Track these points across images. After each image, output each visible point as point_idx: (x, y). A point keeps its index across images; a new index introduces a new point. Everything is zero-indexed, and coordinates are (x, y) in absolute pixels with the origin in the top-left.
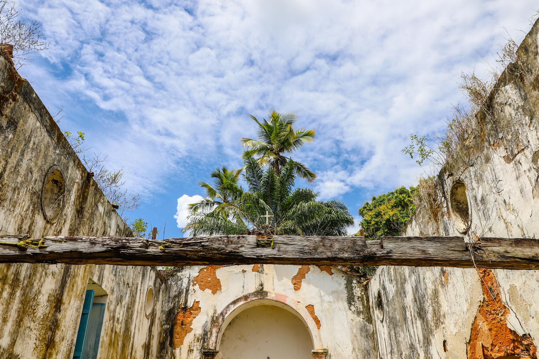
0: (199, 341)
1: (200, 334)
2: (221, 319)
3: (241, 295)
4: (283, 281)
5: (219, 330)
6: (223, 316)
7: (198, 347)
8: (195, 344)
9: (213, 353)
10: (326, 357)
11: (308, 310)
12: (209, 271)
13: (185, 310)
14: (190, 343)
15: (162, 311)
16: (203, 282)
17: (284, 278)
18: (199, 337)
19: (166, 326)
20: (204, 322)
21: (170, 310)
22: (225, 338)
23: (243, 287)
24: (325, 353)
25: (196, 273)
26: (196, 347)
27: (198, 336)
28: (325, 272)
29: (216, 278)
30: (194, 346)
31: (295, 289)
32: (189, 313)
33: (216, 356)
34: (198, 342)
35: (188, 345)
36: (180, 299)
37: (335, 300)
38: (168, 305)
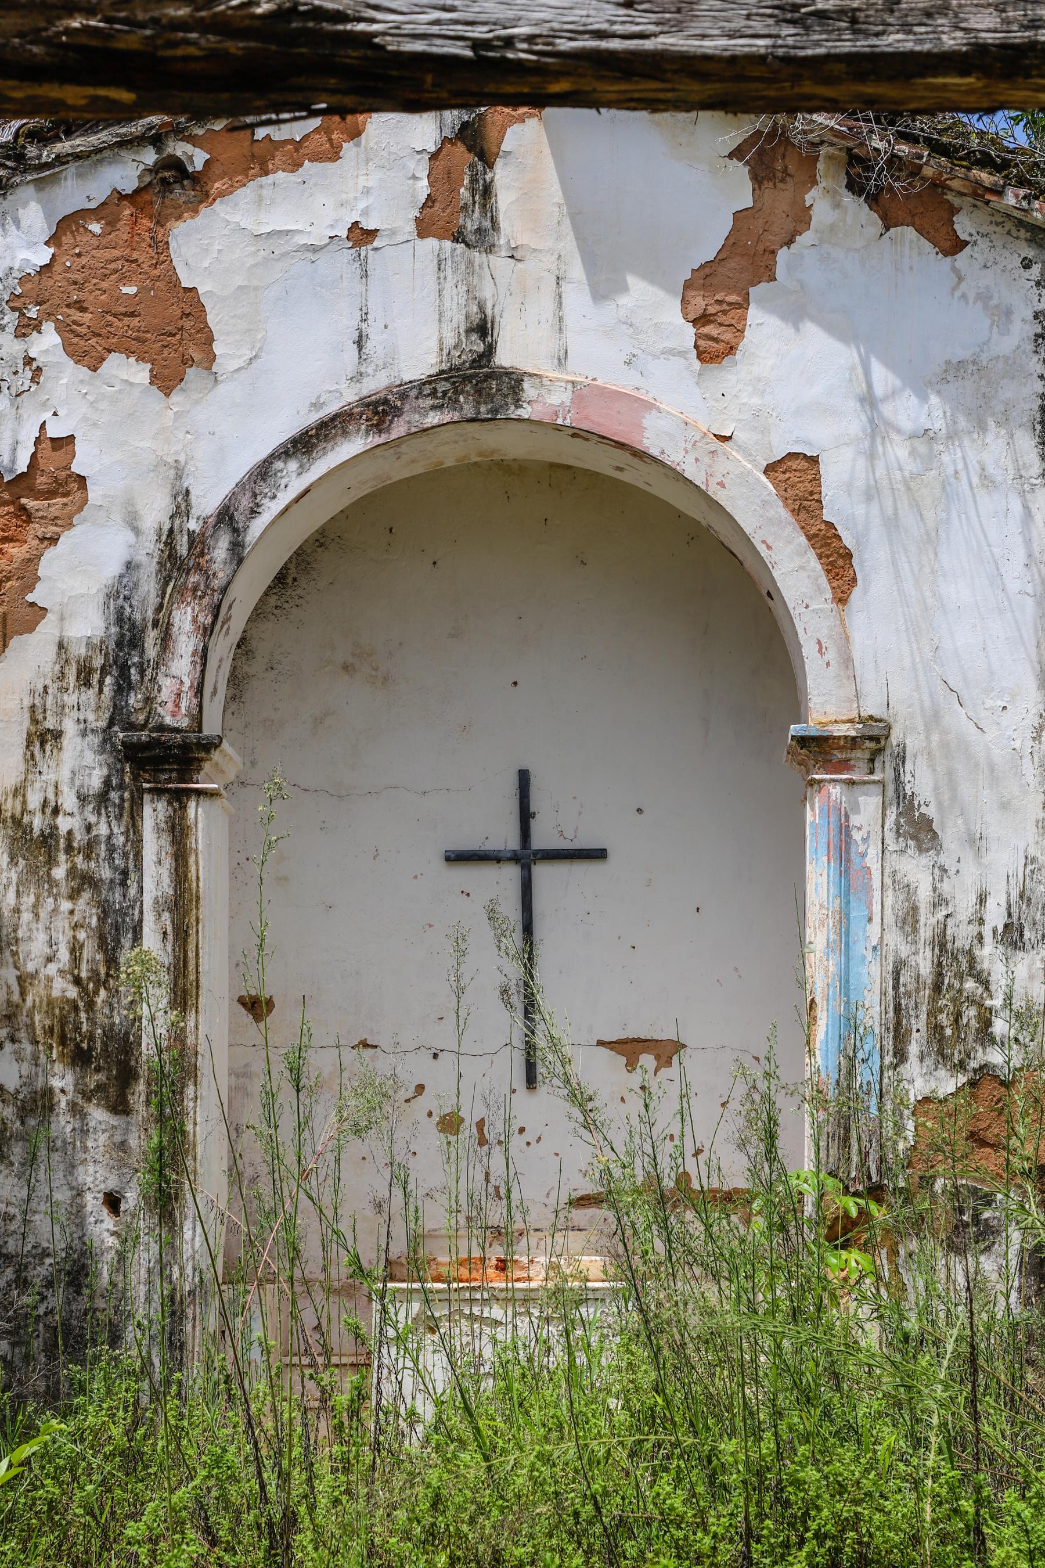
0: (95, 682)
1: (96, 641)
2: (220, 551)
3: (349, 396)
4: (624, 300)
5: (216, 617)
6: (236, 531)
7: (91, 717)
8: (71, 699)
9: (185, 747)
10: (872, 760)
11: (784, 488)
12: (123, 233)
14: (32, 692)
16: (83, 310)
17: (631, 280)
18: (88, 659)
20: (114, 568)
22: (256, 667)
23: (360, 343)
24: (871, 738)
25: (31, 245)
26: (75, 714)
27: (83, 651)
28: (909, 233)
29: (174, 282)
30: (61, 710)
31: (702, 355)
32: (17, 517)
33: (207, 766)
34: (88, 684)
35: (27, 703)
37: (963, 423)
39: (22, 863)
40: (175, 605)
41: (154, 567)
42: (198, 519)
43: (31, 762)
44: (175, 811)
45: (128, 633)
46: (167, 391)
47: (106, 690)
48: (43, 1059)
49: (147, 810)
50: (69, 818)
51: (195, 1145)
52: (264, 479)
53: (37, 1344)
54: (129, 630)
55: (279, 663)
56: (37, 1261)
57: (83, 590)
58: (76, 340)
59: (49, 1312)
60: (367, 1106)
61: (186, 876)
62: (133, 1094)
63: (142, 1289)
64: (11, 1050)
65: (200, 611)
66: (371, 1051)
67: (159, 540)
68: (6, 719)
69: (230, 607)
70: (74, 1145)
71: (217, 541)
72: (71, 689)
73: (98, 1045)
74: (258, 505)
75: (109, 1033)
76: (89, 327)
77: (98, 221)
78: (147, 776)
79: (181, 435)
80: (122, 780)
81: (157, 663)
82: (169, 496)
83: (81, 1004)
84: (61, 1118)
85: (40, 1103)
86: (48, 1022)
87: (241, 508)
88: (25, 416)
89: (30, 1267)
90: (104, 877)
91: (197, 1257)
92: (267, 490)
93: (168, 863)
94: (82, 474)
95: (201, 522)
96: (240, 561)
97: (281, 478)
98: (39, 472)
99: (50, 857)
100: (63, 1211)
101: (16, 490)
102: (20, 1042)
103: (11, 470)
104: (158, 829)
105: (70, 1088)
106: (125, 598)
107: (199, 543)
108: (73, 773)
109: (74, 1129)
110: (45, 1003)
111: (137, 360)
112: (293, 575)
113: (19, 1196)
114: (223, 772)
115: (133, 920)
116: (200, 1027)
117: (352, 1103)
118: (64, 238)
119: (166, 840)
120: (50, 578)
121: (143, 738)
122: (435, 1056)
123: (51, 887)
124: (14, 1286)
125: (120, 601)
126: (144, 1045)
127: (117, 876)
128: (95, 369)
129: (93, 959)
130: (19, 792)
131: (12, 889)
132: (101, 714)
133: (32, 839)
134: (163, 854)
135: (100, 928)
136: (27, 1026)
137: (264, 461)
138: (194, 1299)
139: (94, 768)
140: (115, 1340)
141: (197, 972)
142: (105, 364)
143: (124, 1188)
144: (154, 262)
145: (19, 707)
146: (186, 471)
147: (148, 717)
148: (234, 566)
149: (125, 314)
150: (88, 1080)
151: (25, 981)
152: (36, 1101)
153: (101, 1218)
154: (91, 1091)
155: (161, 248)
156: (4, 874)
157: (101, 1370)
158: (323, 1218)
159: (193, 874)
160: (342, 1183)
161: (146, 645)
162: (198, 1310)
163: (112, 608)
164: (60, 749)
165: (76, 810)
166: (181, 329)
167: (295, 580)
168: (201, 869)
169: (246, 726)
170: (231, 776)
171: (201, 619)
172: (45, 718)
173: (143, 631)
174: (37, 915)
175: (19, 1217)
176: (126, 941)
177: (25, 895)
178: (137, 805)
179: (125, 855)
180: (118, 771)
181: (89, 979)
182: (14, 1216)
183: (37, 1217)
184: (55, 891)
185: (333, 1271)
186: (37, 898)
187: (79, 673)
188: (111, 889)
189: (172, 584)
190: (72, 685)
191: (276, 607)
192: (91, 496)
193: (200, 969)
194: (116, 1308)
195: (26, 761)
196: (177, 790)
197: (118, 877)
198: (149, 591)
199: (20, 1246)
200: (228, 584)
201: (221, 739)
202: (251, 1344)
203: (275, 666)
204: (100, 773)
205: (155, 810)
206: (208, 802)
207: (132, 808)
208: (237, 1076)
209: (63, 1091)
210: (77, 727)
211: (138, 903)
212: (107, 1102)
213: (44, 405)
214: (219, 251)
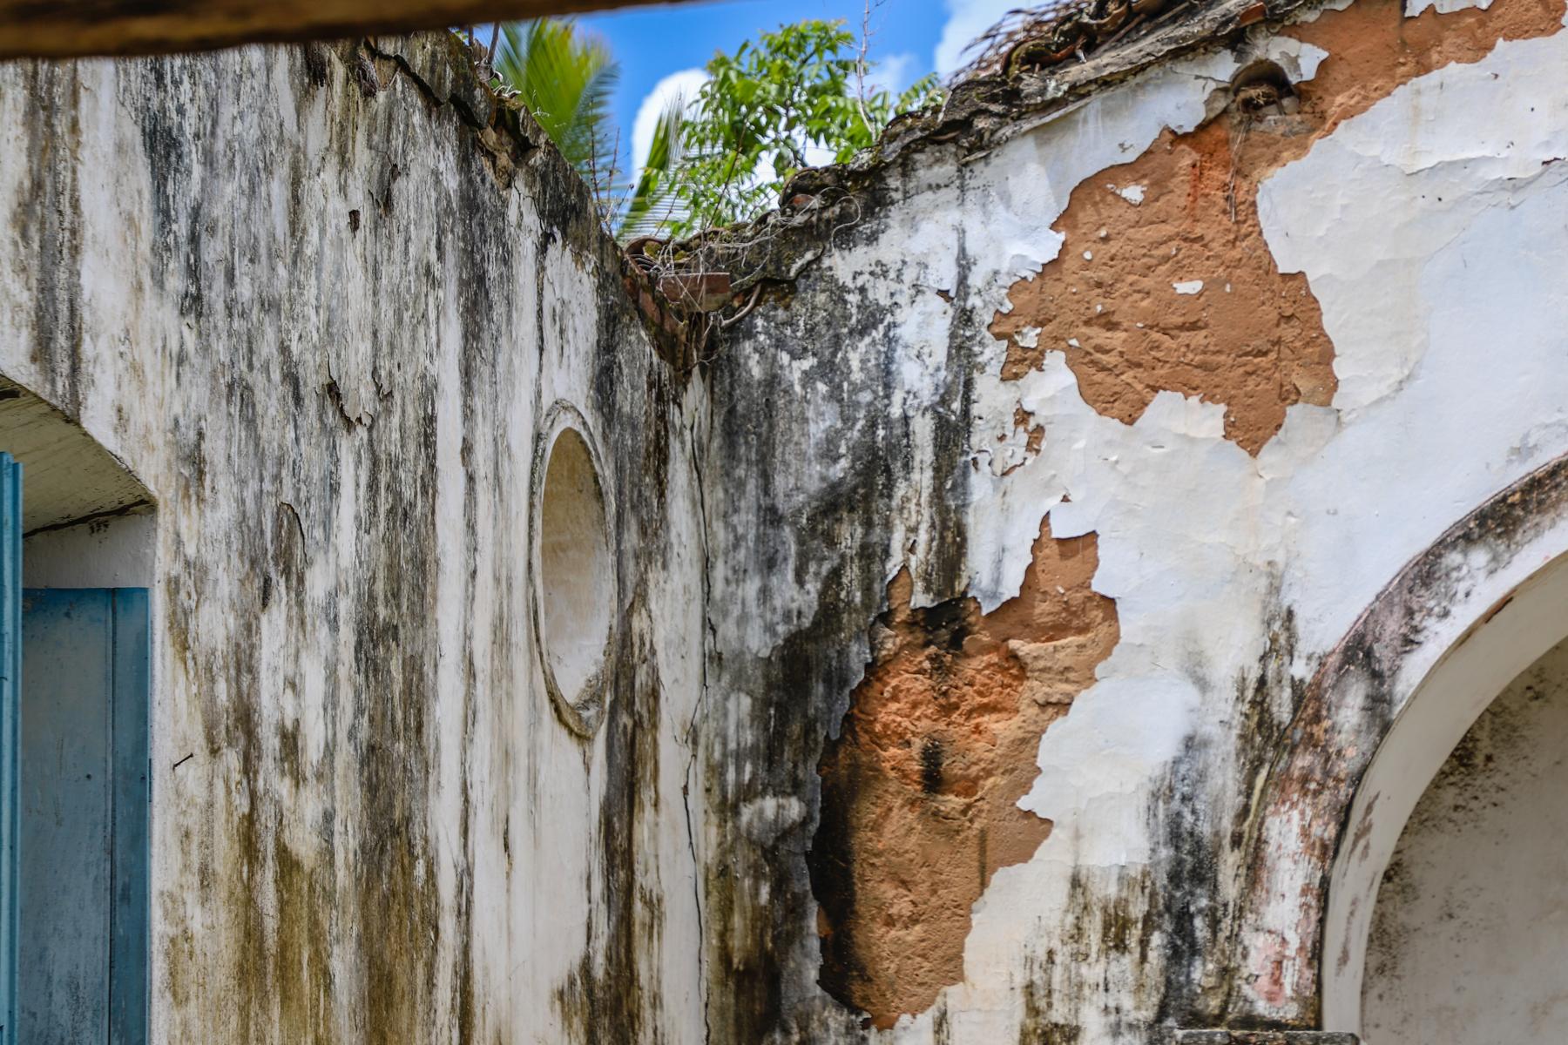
1: (1135, 872)
2: (1349, 711)
5: (1343, 826)
6: (1376, 676)
7: (1127, 1002)
8: (1092, 972)
13: (944, 634)
14: (1029, 961)
16: (1112, 326)
18: (1122, 903)
19: (769, 805)
20: (1164, 749)
21: (791, 640)
22: (1421, 914)
25: (1028, 232)
26: (1100, 999)
27: (1112, 890)
30: (1077, 991)
32: (1004, 670)
34: (1121, 946)
35: (1020, 979)
36: (888, 526)
38: (765, 593)
40: (1271, 808)
41: (1232, 742)
42: (1309, 658)
45: (1189, 858)
46: (1253, 447)
47: (1153, 955)
54: (1191, 853)
55: (1462, 906)
58: (1100, 376)
65: (1316, 816)
69: (1369, 808)
71: (1343, 694)
72: (1094, 955)
74: (1416, 630)
76: (1121, 354)
77: (1137, 181)
81: (1241, 909)
87: (1386, 637)
92: (1432, 603)
94: (1110, 595)
95: (1314, 664)
96: (1386, 728)
97: (1458, 580)
98: (1039, 596)
101: (1002, 627)
103: (994, 595)
107: (1310, 701)
111: (1202, 401)
118: (1081, 215)
121: (1218, 1038)
125: (1176, 804)
128: (1130, 420)
132: (1144, 997)
137: (1427, 554)
142: (1148, 411)
144: (1232, 237)
145: (1007, 986)
148: (1374, 737)
149: (1182, 328)
155: (1243, 213)
161: (1220, 878)
166: (1278, 342)
167: (1489, 758)
169: (1405, 1020)
171: (1317, 830)
172: (1050, 1005)
173: (1215, 854)
187: (1107, 927)
189: (1264, 773)
190: (1094, 949)
191: (1456, 808)
192: (1124, 629)
198: (1224, 785)
200: (1364, 769)
203: (1456, 911)
210: (1103, 1020)
213: (1047, 486)
214: (1344, 207)
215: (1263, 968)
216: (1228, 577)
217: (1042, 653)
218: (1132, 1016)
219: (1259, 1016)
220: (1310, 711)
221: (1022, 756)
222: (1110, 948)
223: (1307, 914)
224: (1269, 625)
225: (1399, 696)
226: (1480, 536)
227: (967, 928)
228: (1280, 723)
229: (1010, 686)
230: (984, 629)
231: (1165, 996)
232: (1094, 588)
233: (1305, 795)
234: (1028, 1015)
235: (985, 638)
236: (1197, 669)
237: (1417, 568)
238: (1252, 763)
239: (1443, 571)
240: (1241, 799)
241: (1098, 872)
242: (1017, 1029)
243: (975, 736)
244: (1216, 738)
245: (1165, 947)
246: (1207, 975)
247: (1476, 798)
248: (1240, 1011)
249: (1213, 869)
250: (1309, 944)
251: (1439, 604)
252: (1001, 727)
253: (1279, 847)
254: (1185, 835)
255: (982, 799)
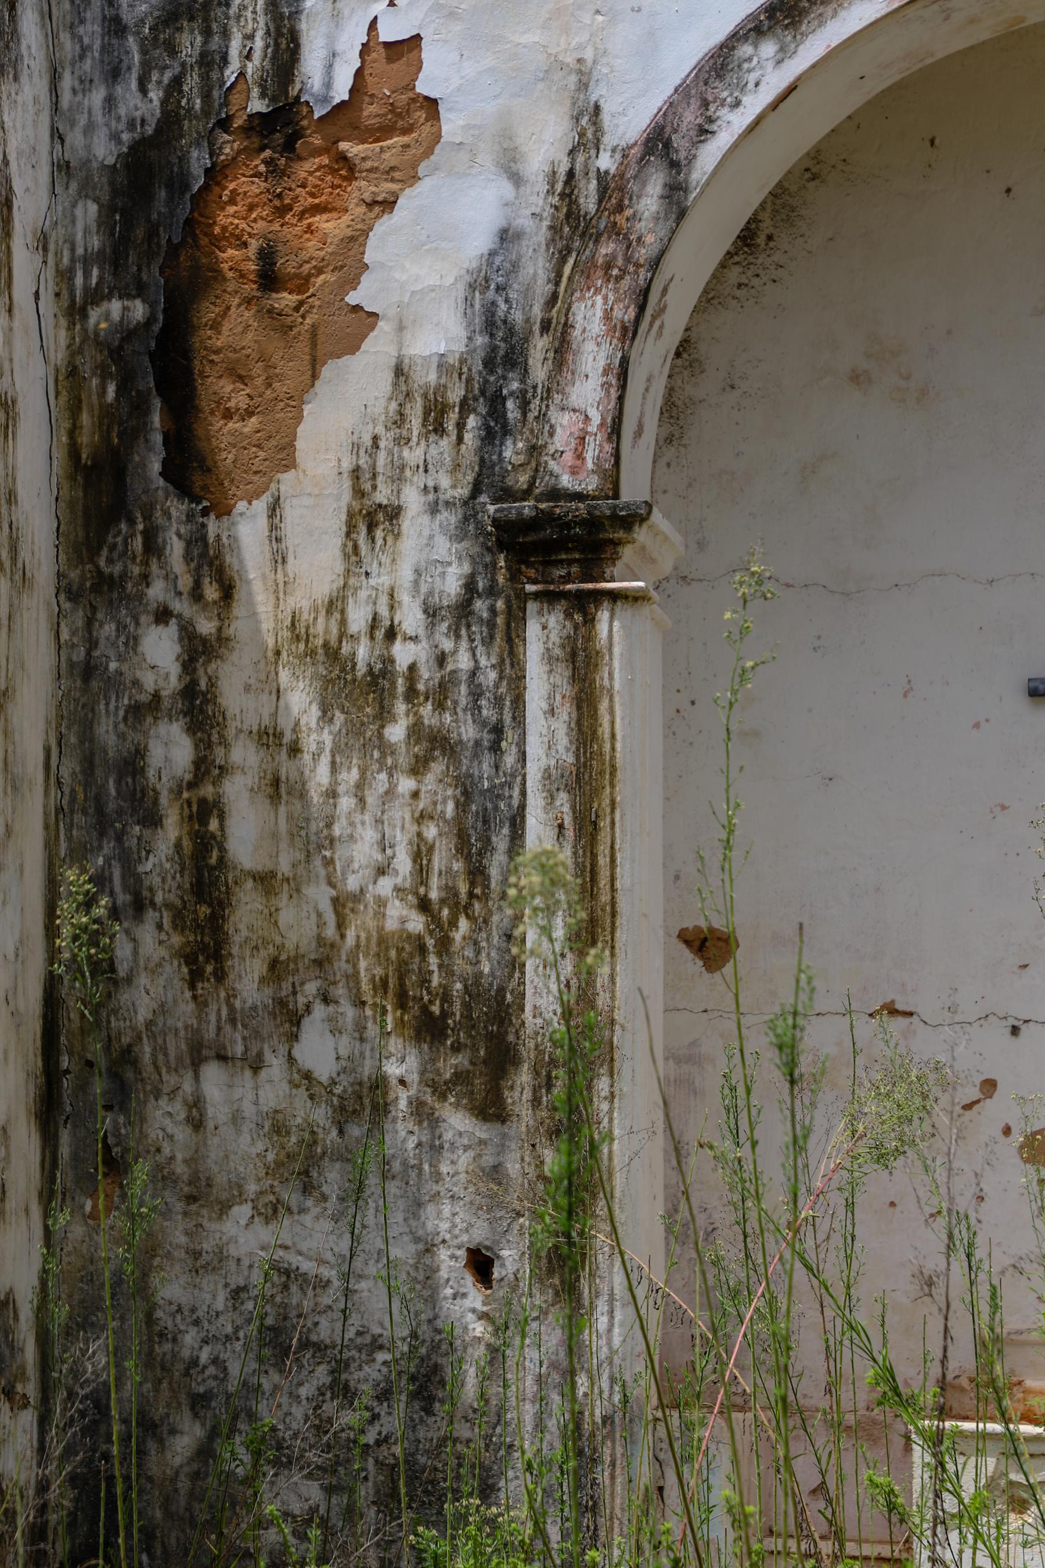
0: (450, 426)
1: (453, 360)
5: (642, 308)
6: (674, 165)
7: (445, 482)
8: (413, 455)
9: (593, 523)
13: (279, 138)
14: (356, 447)
15: (62, 168)
18: (441, 389)
19: (115, 307)
21: (135, 147)
26: (420, 479)
27: (432, 377)
30: (399, 474)
32: (334, 172)
33: (627, 553)
34: (439, 430)
35: (347, 465)
36: (226, 34)
38: (110, 102)
39: (339, 717)
40: (577, 294)
42: (614, 151)
43: (354, 558)
44: (576, 627)
45: (502, 345)
47: (468, 437)
48: (372, 1030)
49: (533, 629)
50: (411, 646)
51: (610, 1174)
52: (720, 77)
53: (365, 1492)
56: (364, 1357)
57: (433, 280)
59: (383, 1441)
60: (897, 1113)
61: (595, 732)
62: (512, 1088)
63: (529, 1411)
64: (323, 1015)
66: (901, 1022)
67: (550, 192)
68: (316, 491)
69: (665, 291)
70: (420, 1170)
71: (644, 184)
72: (415, 439)
73: (457, 1008)
74: (710, 120)
75: (474, 989)
78: (532, 573)
79: (587, 18)
80: (493, 580)
81: (549, 390)
82: (567, 118)
83: (430, 942)
84: (400, 1126)
85: (367, 1101)
86: (379, 971)
88: (346, 12)
89: (353, 1366)
90: (465, 737)
91: (617, 1360)
93: (566, 711)
94: (432, 96)
95: (618, 156)
96: (682, 215)
97: (749, 71)
98: (367, 99)
99: (382, 707)
100: (404, 1276)
102: (337, 1002)
103: (325, 99)
104: (550, 658)
105: (414, 1078)
106: (499, 289)
108: (418, 572)
109: (419, 1144)
110: (374, 941)
112: (767, 231)
113: (336, 1249)
114: (653, 561)
115: (510, 805)
116: (618, 980)
117: (871, 1108)
119: (562, 675)
120: (382, 265)
121: (526, 511)
122: (1015, 1031)
123: (383, 755)
124: (328, 1395)
125: (491, 294)
126: (528, 1008)
127: (485, 735)
129: (449, 870)
130: (336, 605)
131: (325, 760)
132: (460, 476)
133: (354, 680)
134: (558, 697)
135: (458, 819)
136: (347, 977)
137: (722, 46)
138: (612, 1431)
139: (449, 564)
140: (487, 1491)
141: (613, 890)
143: (498, 1242)
145: (335, 471)
146: (595, 75)
147: (533, 480)
150: (441, 1064)
151: (344, 906)
152: (361, 1098)
153: (463, 1290)
154: (446, 1083)
156: (314, 736)
157: (468, 1538)
158: (827, 1300)
159: (605, 730)
160: (858, 1245)
161: (531, 362)
162: (619, 1450)
163: (477, 306)
164: (397, 536)
165: (421, 632)
167: (770, 238)
168: (618, 720)
170: (666, 567)
171: (617, 313)
172: (374, 487)
173: (526, 340)
174: (362, 801)
175: (336, 1283)
176: (501, 841)
177: (344, 769)
178: (516, 619)
179: (498, 702)
180: (486, 566)
181: (443, 901)
182: (329, 1281)
183: (363, 1285)
184: (389, 761)
185: (846, 1395)
186: (363, 772)
187: (427, 413)
188: (475, 756)
189: (571, 261)
190: (415, 433)
191: (740, 286)
192: (445, 128)
193: (618, 885)
194: (488, 1438)
195: (346, 556)
196: (580, 595)
197: (487, 737)
198: (535, 274)
199: (338, 1331)
200: (662, 253)
201: (649, 506)
202: (709, 1510)
204: (458, 571)
205: (544, 628)
206: (629, 612)
207: (508, 625)
208: (678, 1061)
209: (402, 1082)
210: (423, 499)
211: (519, 779)
212: (471, 1100)
215: (568, 444)
216: (541, 75)
217: (370, 153)
218: (449, 494)
219: (563, 489)
220: (614, 201)
221: (350, 253)
222: (429, 432)
223: (608, 392)
224: (577, 120)
225: (694, 183)
226: (770, 28)
227: (299, 418)
228: (586, 214)
229: (340, 186)
230: (315, 132)
231: (479, 474)
232: (418, 90)
233: (608, 280)
234: (354, 498)
235: (317, 141)
236: (512, 164)
237: (712, 61)
238: (560, 252)
239: (736, 63)
240: (550, 287)
241: (419, 361)
242: (345, 509)
243: (307, 236)
244: (528, 230)
245: (479, 429)
246: (517, 454)
247: (758, 276)
248: (547, 485)
249: (524, 354)
250: (609, 420)
251: (731, 95)
252: (332, 226)
253: (584, 331)
254: (499, 323)
255: (314, 295)
